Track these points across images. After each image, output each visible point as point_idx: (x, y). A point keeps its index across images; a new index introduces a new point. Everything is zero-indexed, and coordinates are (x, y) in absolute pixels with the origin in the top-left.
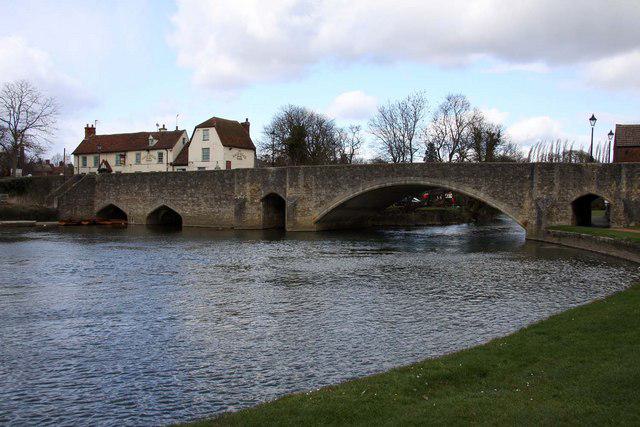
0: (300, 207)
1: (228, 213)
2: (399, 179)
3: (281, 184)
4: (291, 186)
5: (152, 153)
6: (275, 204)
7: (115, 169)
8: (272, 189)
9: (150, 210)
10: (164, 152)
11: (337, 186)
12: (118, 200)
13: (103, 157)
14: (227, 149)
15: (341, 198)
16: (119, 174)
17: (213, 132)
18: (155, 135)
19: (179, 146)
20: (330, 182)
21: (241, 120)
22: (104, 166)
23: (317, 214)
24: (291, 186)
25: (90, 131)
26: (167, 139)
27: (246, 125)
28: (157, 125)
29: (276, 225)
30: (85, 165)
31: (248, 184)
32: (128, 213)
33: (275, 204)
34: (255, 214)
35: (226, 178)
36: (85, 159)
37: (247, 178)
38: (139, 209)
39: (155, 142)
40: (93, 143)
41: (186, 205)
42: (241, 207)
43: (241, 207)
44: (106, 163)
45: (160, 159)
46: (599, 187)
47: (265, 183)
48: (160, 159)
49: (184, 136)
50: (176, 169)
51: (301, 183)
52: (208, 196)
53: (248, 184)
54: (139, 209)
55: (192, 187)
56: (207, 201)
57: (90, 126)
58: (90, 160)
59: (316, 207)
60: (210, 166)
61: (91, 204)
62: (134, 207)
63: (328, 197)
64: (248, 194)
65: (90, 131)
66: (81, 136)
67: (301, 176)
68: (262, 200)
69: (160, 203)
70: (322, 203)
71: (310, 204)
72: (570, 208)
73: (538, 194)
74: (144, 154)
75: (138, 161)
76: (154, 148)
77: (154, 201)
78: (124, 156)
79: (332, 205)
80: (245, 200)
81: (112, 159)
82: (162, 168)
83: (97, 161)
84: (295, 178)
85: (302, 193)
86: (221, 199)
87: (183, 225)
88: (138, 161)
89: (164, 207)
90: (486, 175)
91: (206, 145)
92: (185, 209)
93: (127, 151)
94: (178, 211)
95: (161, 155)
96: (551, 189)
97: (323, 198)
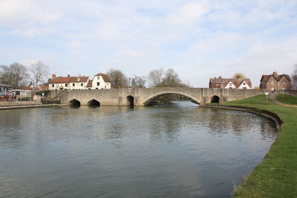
1: (116, 101)
11: (149, 93)
34: (125, 101)
38: (84, 100)
39: (80, 80)
43: (120, 99)
52: (109, 96)
56: (108, 98)
59: (143, 99)
60: (100, 88)
61: (67, 99)
63: (147, 96)
70: (145, 98)
74: (76, 84)
76: (79, 82)
91: (98, 81)
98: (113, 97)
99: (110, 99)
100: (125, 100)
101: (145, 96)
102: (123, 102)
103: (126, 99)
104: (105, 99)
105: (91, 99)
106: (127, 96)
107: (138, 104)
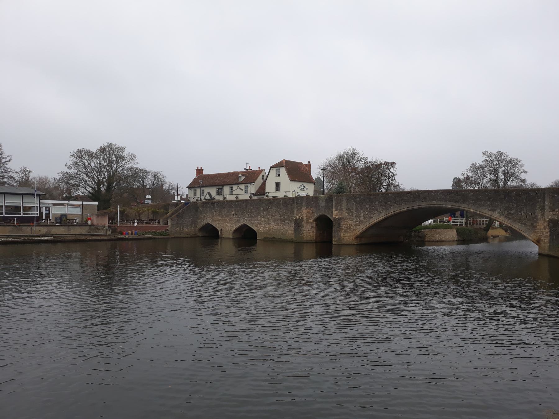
0: (343, 225)
1: (289, 230)
2: (424, 203)
3: (329, 207)
4: (336, 210)
6: (325, 225)
8: (322, 212)
9: (235, 228)
10: (249, 185)
15: (379, 216)
17: (283, 171)
19: (259, 181)
22: (208, 197)
25: (199, 171)
27: (309, 165)
29: (325, 242)
30: (195, 195)
32: (219, 230)
33: (325, 225)
34: (309, 231)
35: (290, 203)
36: (195, 191)
37: (304, 204)
38: (227, 226)
39: (243, 178)
40: (202, 180)
41: (260, 224)
43: (298, 224)
44: (209, 194)
45: (246, 191)
47: (317, 207)
48: (246, 191)
49: (262, 174)
54: (227, 226)
55: (264, 210)
56: (274, 221)
57: (199, 168)
58: (198, 191)
59: (356, 225)
62: (224, 225)
64: (304, 215)
65: (199, 171)
66: (194, 175)
68: (314, 220)
69: (242, 222)
71: (352, 225)
74: (235, 187)
75: (231, 191)
77: (238, 221)
78: (221, 189)
79: (368, 224)
80: (302, 220)
81: (213, 191)
83: (202, 193)
85: (345, 214)
86: (284, 220)
88: (231, 191)
89: (245, 226)
91: (278, 180)
92: (261, 226)
93: (223, 185)
94: (255, 229)
95: (246, 187)
98: (284, 220)
99: (278, 225)
100: (312, 227)
101: (358, 216)
102: (305, 233)
103: (314, 224)
104: (269, 224)
105: (239, 225)
106: (316, 216)
107: (340, 239)
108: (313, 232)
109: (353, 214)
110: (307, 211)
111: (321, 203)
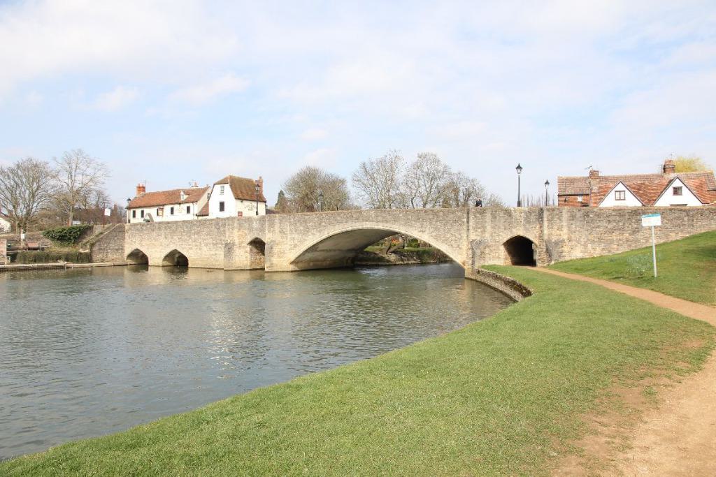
0: (276, 250)
3: (262, 230)
5: (182, 205)
7: (156, 219)
12: (141, 246)
13: (147, 211)
14: (239, 202)
16: (160, 223)
18: (187, 192)
20: (302, 228)
21: (255, 178)
23: (293, 255)
24: (269, 231)
26: (195, 195)
28: (190, 184)
31: (235, 231)
37: (235, 225)
39: (186, 197)
42: (229, 248)
43: (229, 248)
44: (149, 215)
46: (526, 229)
47: (251, 229)
50: (200, 218)
51: (277, 227)
53: (235, 231)
56: (206, 245)
57: (141, 186)
67: (277, 221)
70: (295, 246)
72: (502, 248)
73: (473, 236)
74: (176, 207)
80: (234, 244)
81: (153, 211)
82: (190, 217)
84: (272, 225)
87: (189, 266)
90: (430, 219)
93: (164, 205)
96: (484, 231)
97: (296, 242)
102: (237, 259)
104: (200, 249)
108: (246, 257)
109: (287, 237)
110: (240, 233)
111: (255, 225)
